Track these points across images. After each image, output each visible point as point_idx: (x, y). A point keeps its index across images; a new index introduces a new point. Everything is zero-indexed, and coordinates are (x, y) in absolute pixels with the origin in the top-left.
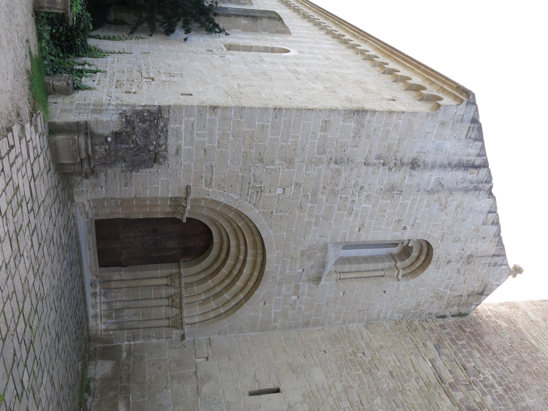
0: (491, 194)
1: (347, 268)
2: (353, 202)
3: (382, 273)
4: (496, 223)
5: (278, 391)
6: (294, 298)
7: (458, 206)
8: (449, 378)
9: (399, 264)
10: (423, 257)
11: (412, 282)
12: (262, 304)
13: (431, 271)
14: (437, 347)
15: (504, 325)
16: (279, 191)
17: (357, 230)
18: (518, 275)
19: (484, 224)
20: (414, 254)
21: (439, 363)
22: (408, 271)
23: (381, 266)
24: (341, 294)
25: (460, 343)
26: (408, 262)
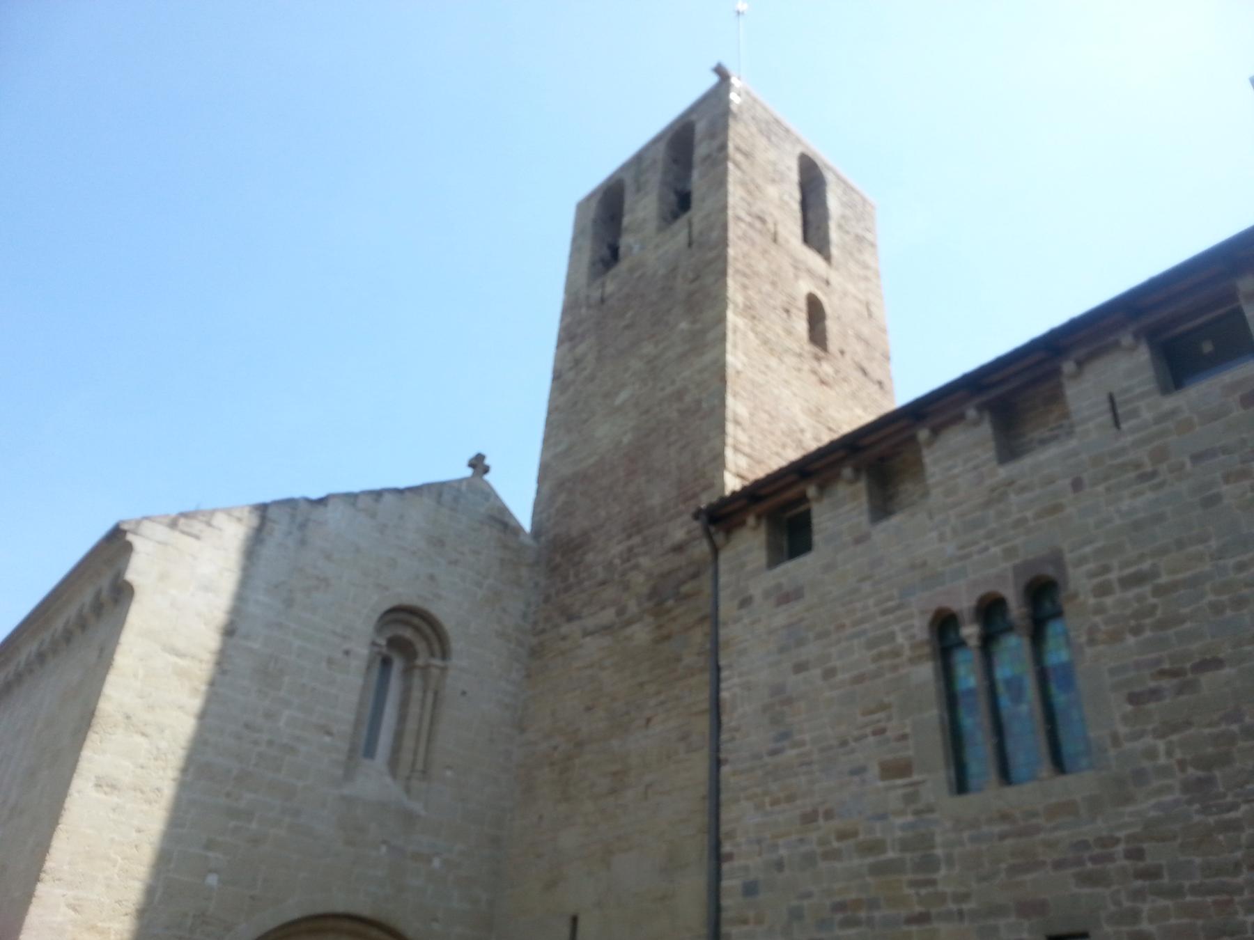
0: (322, 501)
1: (406, 756)
2: (270, 743)
3: (430, 696)
4: (378, 494)
5: (575, 920)
6: (436, 863)
7: (328, 557)
8: (608, 615)
9: (420, 662)
10: (416, 621)
11: (457, 644)
12: (436, 926)
13: (442, 611)
14: (570, 618)
15: (562, 498)
16: (212, 880)
17: (327, 739)
18: (487, 462)
19: (373, 516)
20: (408, 633)
21: (590, 623)
22: (436, 647)
23: (416, 694)
24: (449, 773)
25: (572, 579)
26: (421, 646)
